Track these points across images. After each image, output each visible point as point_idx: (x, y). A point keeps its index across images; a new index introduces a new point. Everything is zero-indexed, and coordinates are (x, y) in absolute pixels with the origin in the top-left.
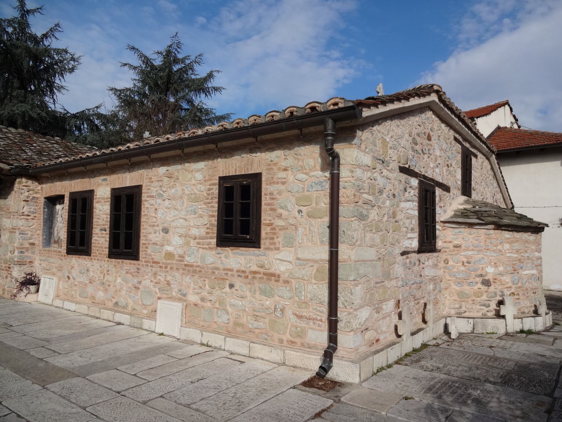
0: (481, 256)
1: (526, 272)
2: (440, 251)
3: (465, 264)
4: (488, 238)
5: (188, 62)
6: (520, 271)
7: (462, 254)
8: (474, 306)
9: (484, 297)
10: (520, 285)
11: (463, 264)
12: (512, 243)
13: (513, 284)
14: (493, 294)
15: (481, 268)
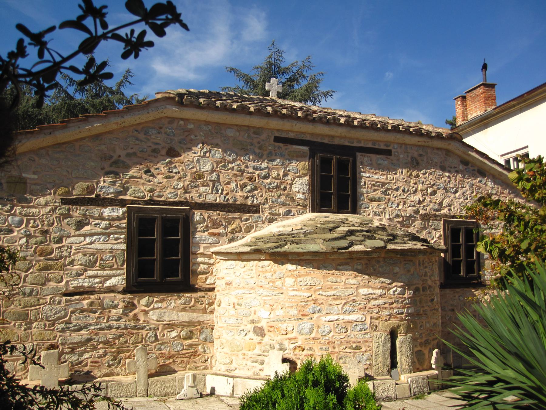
0: (253, 295)
1: (328, 318)
2: (213, 289)
3: (237, 307)
4: (262, 271)
5: (295, 69)
6: (315, 316)
7: (233, 293)
8: (245, 362)
9: (257, 351)
10: (313, 335)
11: (234, 307)
12: (299, 276)
13: (301, 334)
14: (268, 347)
15: (253, 313)
